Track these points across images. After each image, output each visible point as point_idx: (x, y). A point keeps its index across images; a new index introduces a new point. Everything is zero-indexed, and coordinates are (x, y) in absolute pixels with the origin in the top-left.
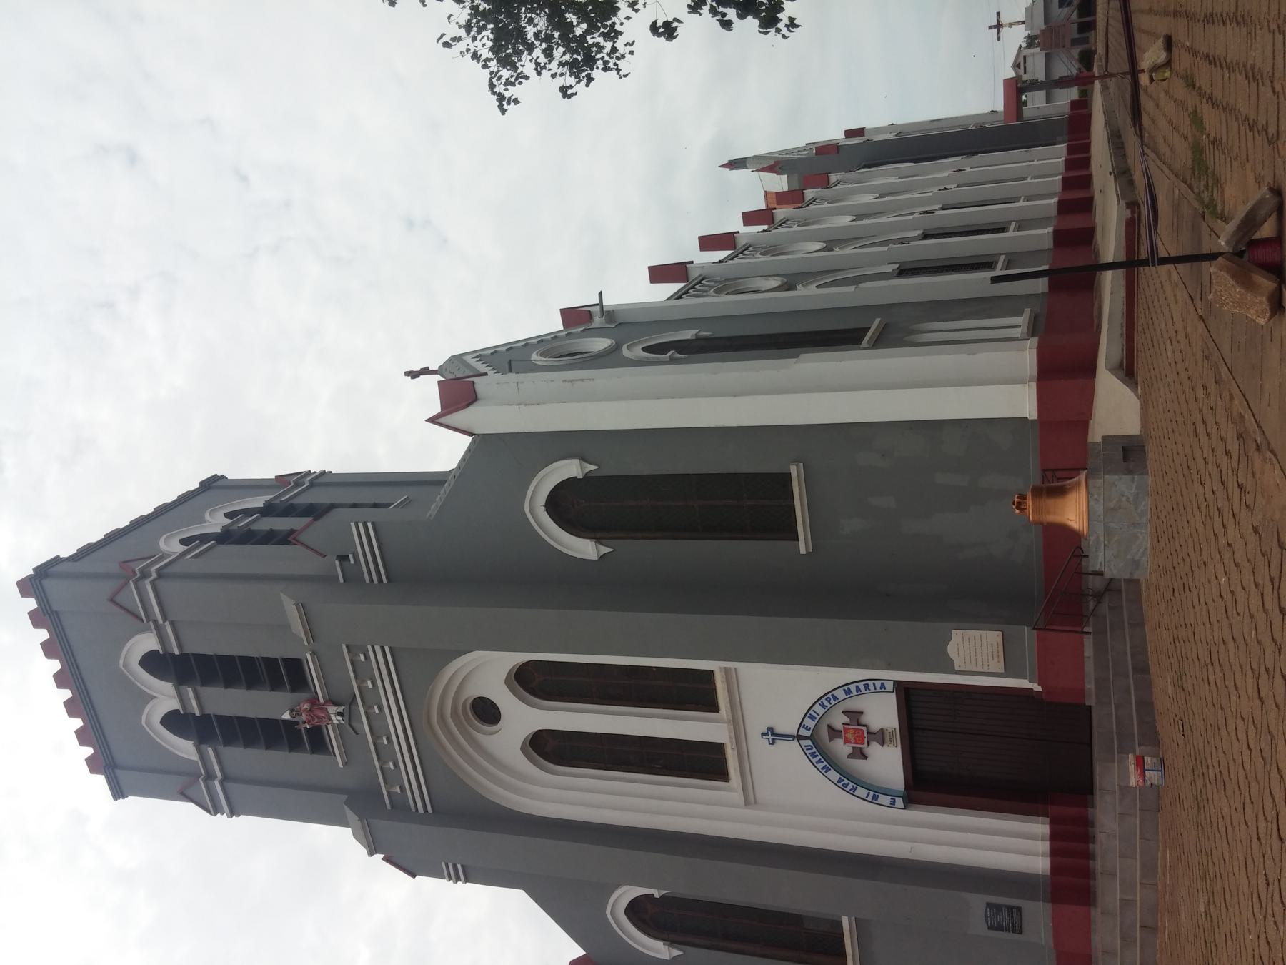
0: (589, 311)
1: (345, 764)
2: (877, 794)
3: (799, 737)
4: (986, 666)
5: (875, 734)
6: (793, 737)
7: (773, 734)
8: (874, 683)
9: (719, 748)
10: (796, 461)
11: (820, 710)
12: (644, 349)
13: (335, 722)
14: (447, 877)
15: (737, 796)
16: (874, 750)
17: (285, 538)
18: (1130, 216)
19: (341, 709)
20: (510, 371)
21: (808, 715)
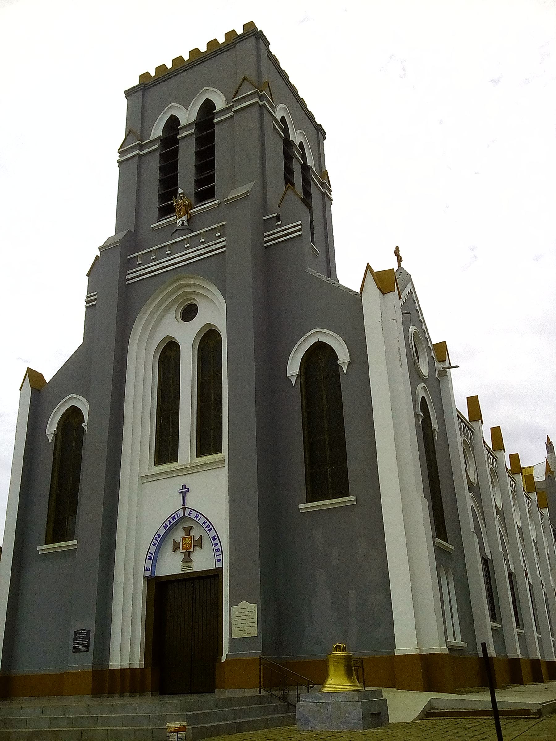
0: (446, 360)
1: (153, 229)
2: (152, 559)
3: (184, 509)
4: (237, 626)
5: (189, 557)
6: (184, 505)
7: (185, 492)
8: (220, 555)
9: (174, 458)
10: (357, 500)
11: (201, 522)
12: (423, 397)
14: (88, 295)
15: (146, 471)
16: (179, 556)
17: (289, 181)
18: (532, 712)
19: (186, 224)
20: (403, 314)
21: (198, 514)
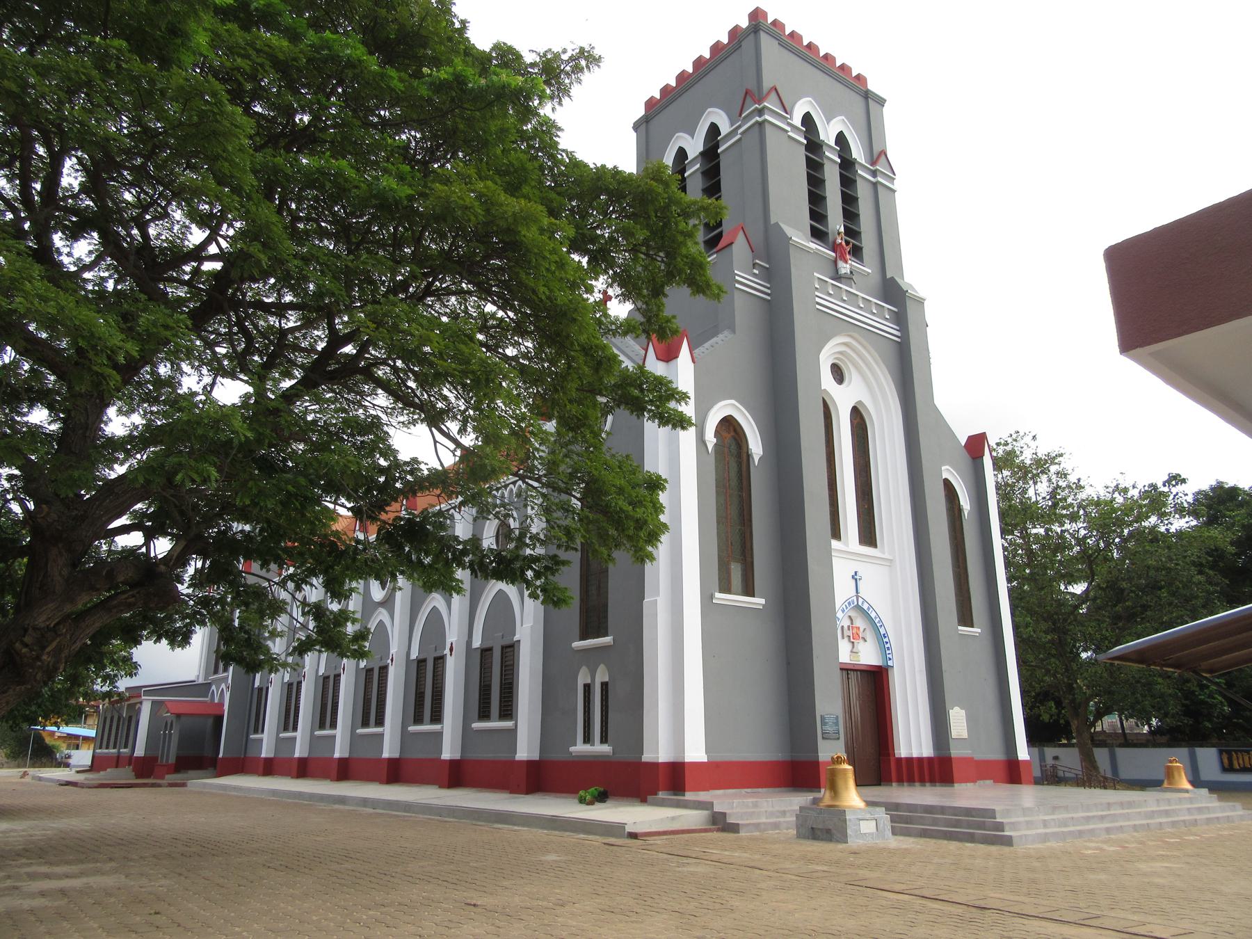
6: (857, 592)
13: (841, 264)
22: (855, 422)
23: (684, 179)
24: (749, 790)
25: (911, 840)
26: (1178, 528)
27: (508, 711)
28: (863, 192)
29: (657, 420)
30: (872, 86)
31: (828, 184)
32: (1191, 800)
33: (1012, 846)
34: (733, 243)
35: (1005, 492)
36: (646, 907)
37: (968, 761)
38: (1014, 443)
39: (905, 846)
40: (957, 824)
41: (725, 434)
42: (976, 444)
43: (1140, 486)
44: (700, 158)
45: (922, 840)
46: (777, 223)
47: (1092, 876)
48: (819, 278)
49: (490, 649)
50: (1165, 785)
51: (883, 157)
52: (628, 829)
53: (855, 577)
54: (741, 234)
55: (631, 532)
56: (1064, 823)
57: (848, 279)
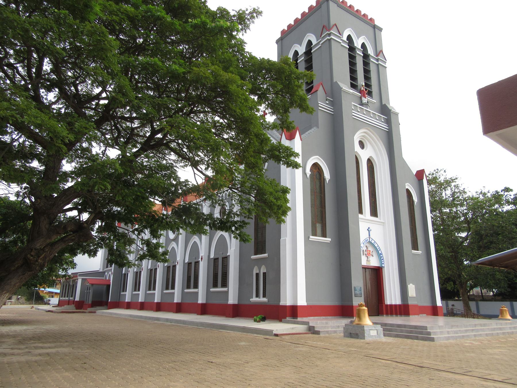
3: (369, 238)
13: (363, 98)
22: (369, 165)
23: (297, 64)
24: (324, 317)
25: (392, 338)
26: (507, 210)
27: (225, 284)
28: (373, 68)
29: (286, 165)
30: (377, 23)
31: (357, 65)
32: (511, 324)
33: (434, 341)
34: (317, 90)
35: (432, 194)
36: (282, 364)
37: (416, 306)
38: (436, 174)
39: (389, 341)
40: (411, 332)
41: (314, 170)
42: (420, 174)
43: (491, 192)
44: (304, 55)
45: (396, 339)
46: (336, 82)
47: (468, 355)
48: (354, 105)
49: (218, 259)
50: (500, 317)
51: (381, 53)
52: (274, 332)
53: (369, 230)
54: (321, 86)
55: (275, 211)
56: (456, 332)
57: (366, 105)
